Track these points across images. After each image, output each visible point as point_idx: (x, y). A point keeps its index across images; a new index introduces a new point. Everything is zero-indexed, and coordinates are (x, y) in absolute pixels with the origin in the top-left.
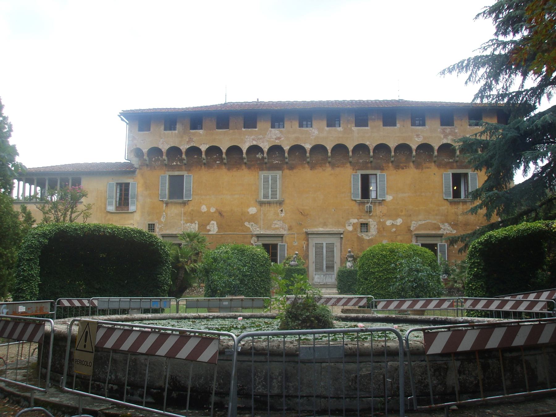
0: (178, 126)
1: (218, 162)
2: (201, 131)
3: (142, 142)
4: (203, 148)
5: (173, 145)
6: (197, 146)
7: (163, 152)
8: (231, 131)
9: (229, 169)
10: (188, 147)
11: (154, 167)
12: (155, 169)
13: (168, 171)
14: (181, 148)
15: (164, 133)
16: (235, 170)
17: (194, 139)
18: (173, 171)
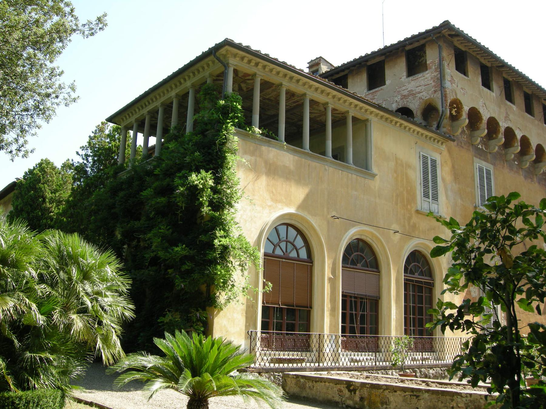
0: (495, 86)
1: (516, 162)
2: (514, 107)
3: (462, 91)
4: (519, 135)
5: (493, 115)
6: (514, 128)
7: (483, 121)
8: (536, 122)
9: (526, 177)
10: (506, 126)
11: (461, 143)
12: (462, 147)
13: (476, 157)
14: (501, 124)
15: (483, 90)
16: (530, 180)
17: (511, 116)
18: (480, 158)
